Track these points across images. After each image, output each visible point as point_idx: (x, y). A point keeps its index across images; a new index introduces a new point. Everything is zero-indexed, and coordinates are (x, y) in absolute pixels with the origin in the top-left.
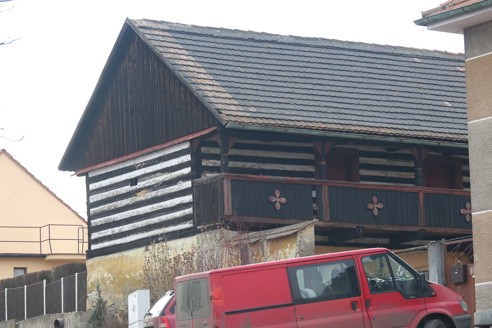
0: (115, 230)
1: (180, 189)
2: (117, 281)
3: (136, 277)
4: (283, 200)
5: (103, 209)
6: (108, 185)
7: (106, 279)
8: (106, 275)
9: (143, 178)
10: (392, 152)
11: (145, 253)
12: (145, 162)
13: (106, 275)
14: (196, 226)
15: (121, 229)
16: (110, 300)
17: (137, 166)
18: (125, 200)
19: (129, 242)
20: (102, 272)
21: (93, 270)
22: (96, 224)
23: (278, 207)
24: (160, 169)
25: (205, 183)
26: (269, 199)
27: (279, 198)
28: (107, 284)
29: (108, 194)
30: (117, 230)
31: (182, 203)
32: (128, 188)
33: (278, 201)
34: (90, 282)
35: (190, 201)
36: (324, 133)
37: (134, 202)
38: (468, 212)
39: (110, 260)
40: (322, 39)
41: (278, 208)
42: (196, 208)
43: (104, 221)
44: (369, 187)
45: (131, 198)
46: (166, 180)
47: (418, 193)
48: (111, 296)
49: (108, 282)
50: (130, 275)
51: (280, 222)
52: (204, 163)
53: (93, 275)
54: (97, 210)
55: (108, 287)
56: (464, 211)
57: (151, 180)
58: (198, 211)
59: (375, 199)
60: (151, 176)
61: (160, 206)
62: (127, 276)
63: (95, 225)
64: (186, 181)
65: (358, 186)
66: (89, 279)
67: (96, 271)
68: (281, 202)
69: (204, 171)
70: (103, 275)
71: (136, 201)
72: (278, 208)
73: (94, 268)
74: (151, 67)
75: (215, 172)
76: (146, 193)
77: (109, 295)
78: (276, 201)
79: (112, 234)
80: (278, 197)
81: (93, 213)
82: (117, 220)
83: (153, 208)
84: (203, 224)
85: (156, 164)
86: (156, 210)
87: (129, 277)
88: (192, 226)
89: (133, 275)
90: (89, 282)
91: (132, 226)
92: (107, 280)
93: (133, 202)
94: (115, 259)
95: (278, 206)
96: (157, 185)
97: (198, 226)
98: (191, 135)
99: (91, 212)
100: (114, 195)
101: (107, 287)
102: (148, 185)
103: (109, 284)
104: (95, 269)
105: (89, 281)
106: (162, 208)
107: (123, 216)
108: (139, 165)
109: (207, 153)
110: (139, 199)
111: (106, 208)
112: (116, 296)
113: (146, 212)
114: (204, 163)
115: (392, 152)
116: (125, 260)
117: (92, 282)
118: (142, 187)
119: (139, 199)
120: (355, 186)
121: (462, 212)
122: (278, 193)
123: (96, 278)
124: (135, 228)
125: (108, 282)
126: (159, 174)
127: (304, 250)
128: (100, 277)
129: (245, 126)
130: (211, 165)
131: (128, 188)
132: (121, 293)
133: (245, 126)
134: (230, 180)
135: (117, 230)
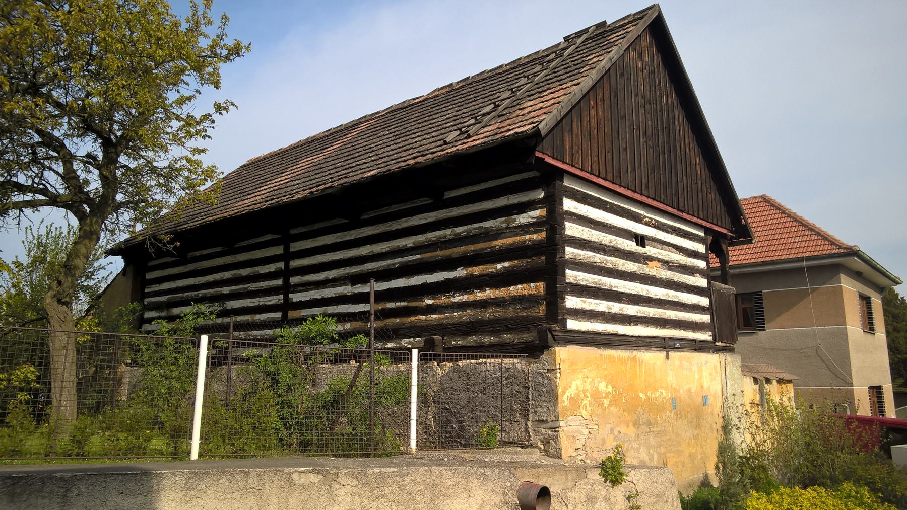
5: (592, 259)
7: (604, 395)
8: (602, 386)
13: (602, 386)
16: (612, 437)
21: (574, 371)
22: (575, 280)
28: (606, 405)
34: (568, 396)
43: (594, 283)
48: (612, 430)
49: (606, 402)
50: (646, 394)
55: (607, 410)
57: (665, 253)
62: (641, 395)
63: (573, 282)
67: (581, 375)
77: (609, 426)
79: (607, 311)
81: (571, 256)
85: (668, 232)
89: (651, 395)
103: (609, 406)
104: (578, 371)
105: (564, 392)
107: (625, 287)
108: (647, 219)
112: (623, 429)
116: (638, 366)
117: (573, 396)
124: (644, 315)
125: (606, 402)
128: (590, 390)
132: (631, 425)
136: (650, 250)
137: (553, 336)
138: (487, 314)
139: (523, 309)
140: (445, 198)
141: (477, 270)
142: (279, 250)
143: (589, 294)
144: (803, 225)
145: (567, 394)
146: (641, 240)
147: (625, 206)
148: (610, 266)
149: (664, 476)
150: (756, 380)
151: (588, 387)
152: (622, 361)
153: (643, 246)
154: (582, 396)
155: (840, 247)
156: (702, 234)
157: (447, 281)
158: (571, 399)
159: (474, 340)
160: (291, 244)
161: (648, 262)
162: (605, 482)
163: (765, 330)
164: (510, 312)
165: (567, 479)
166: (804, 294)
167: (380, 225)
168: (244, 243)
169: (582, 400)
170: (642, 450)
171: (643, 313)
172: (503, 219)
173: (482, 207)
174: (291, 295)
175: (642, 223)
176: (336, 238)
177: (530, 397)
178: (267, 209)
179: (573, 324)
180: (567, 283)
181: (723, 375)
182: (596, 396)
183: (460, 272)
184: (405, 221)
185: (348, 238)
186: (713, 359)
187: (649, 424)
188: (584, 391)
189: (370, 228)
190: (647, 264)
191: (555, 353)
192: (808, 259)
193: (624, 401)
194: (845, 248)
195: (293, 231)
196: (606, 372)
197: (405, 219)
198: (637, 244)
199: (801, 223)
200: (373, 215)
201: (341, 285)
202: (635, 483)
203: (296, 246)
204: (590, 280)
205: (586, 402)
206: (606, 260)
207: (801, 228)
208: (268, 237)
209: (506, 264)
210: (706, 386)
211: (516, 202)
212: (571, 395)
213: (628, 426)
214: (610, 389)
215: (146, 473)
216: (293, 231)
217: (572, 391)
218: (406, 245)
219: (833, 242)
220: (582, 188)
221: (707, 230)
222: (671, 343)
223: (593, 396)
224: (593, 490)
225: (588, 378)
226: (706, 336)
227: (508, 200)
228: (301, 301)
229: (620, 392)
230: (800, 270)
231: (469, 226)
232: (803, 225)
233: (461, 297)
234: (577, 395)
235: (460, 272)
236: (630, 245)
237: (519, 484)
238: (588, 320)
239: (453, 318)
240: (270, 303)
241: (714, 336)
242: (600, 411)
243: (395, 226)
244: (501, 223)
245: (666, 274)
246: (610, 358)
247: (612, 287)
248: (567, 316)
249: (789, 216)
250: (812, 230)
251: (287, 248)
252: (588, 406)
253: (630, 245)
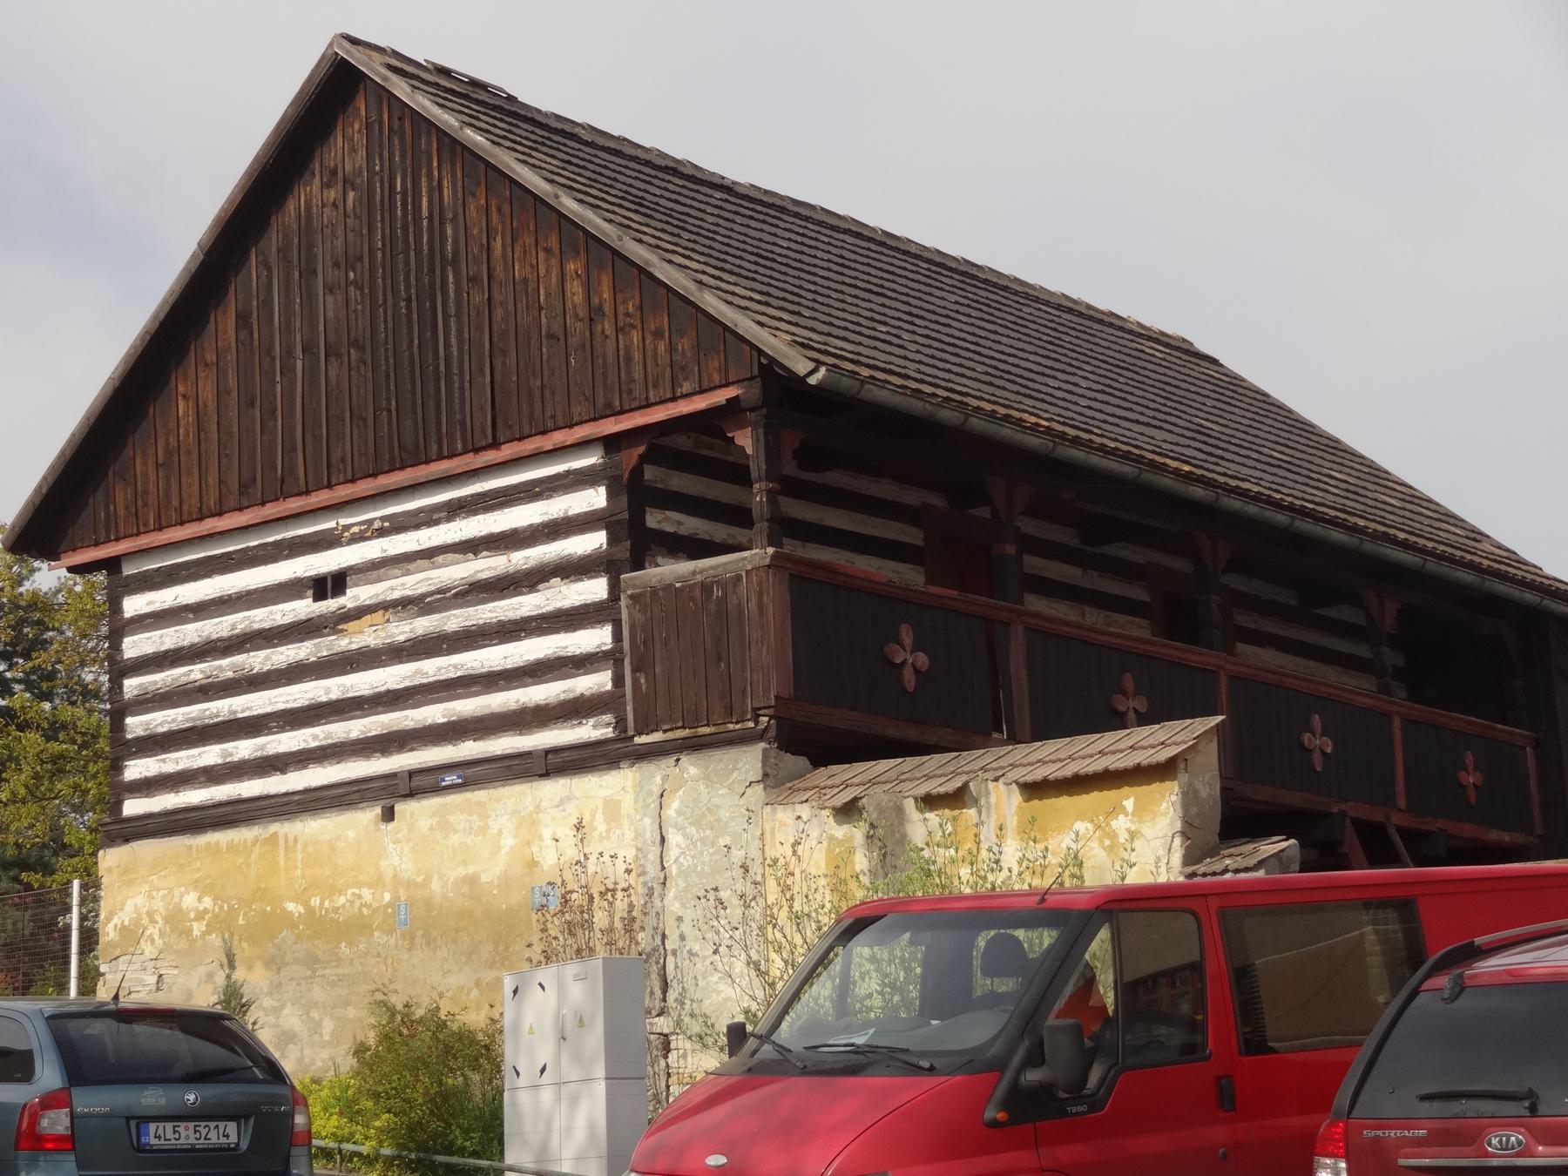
0: (236, 748)
1: (550, 608)
2: (241, 922)
3: (336, 910)
4: (922, 659)
5: (184, 680)
6: (207, 598)
7: (192, 915)
8: (190, 900)
9: (375, 574)
10: (1091, 549)
11: (379, 829)
12: (383, 519)
13: (190, 900)
14: (631, 733)
15: (263, 747)
17: (346, 534)
18: (289, 647)
19: (301, 788)
20: (171, 890)
21: (129, 883)
22: (146, 730)
23: (909, 682)
24: (457, 540)
25: (678, 585)
26: (887, 650)
27: (912, 653)
29: (206, 627)
30: (244, 749)
31: (562, 654)
32: (303, 608)
33: (910, 661)
34: (116, 926)
35: (598, 647)
36: (1051, 444)
37: (331, 652)
38: (1318, 742)
39: (214, 850)
40: (822, 209)
41: (911, 687)
42: (635, 671)
43: (188, 720)
44: (1116, 641)
45: (319, 640)
46: (484, 575)
47: (1215, 672)
49: (198, 928)
50: (306, 904)
51: (912, 734)
52: (655, 519)
53: (129, 902)
54: (155, 683)
55: (200, 943)
56: (1309, 739)
57: (410, 580)
58: (643, 681)
59: (1128, 681)
60: (412, 566)
61: (455, 666)
62: (291, 906)
63: (142, 733)
64: (582, 580)
65: (1093, 635)
68: (918, 666)
69: (653, 547)
70: (176, 899)
71: (337, 649)
72: (911, 687)
73: (137, 879)
74: (425, 200)
75: (680, 554)
76: (388, 621)
78: (904, 663)
79: (220, 761)
80: (909, 649)
81: (135, 692)
82: (247, 714)
83: (418, 672)
84: (665, 727)
85: (437, 522)
86: (431, 680)
87: (302, 911)
88: (611, 735)
89: (322, 903)
90: (111, 926)
91: (315, 737)
92: (196, 919)
93: (325, 654)
94: (232, 847)
95: (909, 677)
96: (439, 596)
97: (640, 734)
98: (613, 418)
99: (125, 690)
100: (236, 632)
101: (195, 940)
102: (396, 595)
103: (204, 934)
104: (138, 881)
105: (109, 919)
106: (459, 674)
107: (273, 700)
109: (659, 486)
110: (351, 643)
111: (194, 676)
113: (383, 689)
114: (655, 519)
115: (1091, 549)
116: (282, 852)
117: (126, 923)
118: (367, 603)
119: (351, 643)
120: (1085, 633)
121: (1306, 743)
122: (907, 637)
123: (146, 909)
124: (330, 741)
125: (198, 928)
126: (450, 557)
127: (1197, 822)
128: (162, 910)
129: (867, 386)
130: (669, 528)
131: (303, 608)
133: (867, 386)
134: (787, 575)
135: (244, 749)
145: (116, 920)
147: (278, 537)
148: (230, 674)
151: (159, 905)
154: (145, 921)
158: (123, 930)
169: (145, 929)
170: (286, 1011)
171: (325, 738)
182: (176, 921)
186: (619, 784)
187: (312, 961)
188: (150, 914)
193: (241, 922)
204: (180, 718)
205: (153, 931)
206: (220, 667)
212: (123, 921)
214: (207, 902)
217: (125, 916)
220: (163, 561)
222: (427, 780)
223: (167, 920)
225: (159, 890)
229: (231, 908)
234: (136, 922)
238: (171, 791)
241: (620, 724)
242: (183, 944)
245: (403, 630)
247: (235, 712)
252: (156, 937)
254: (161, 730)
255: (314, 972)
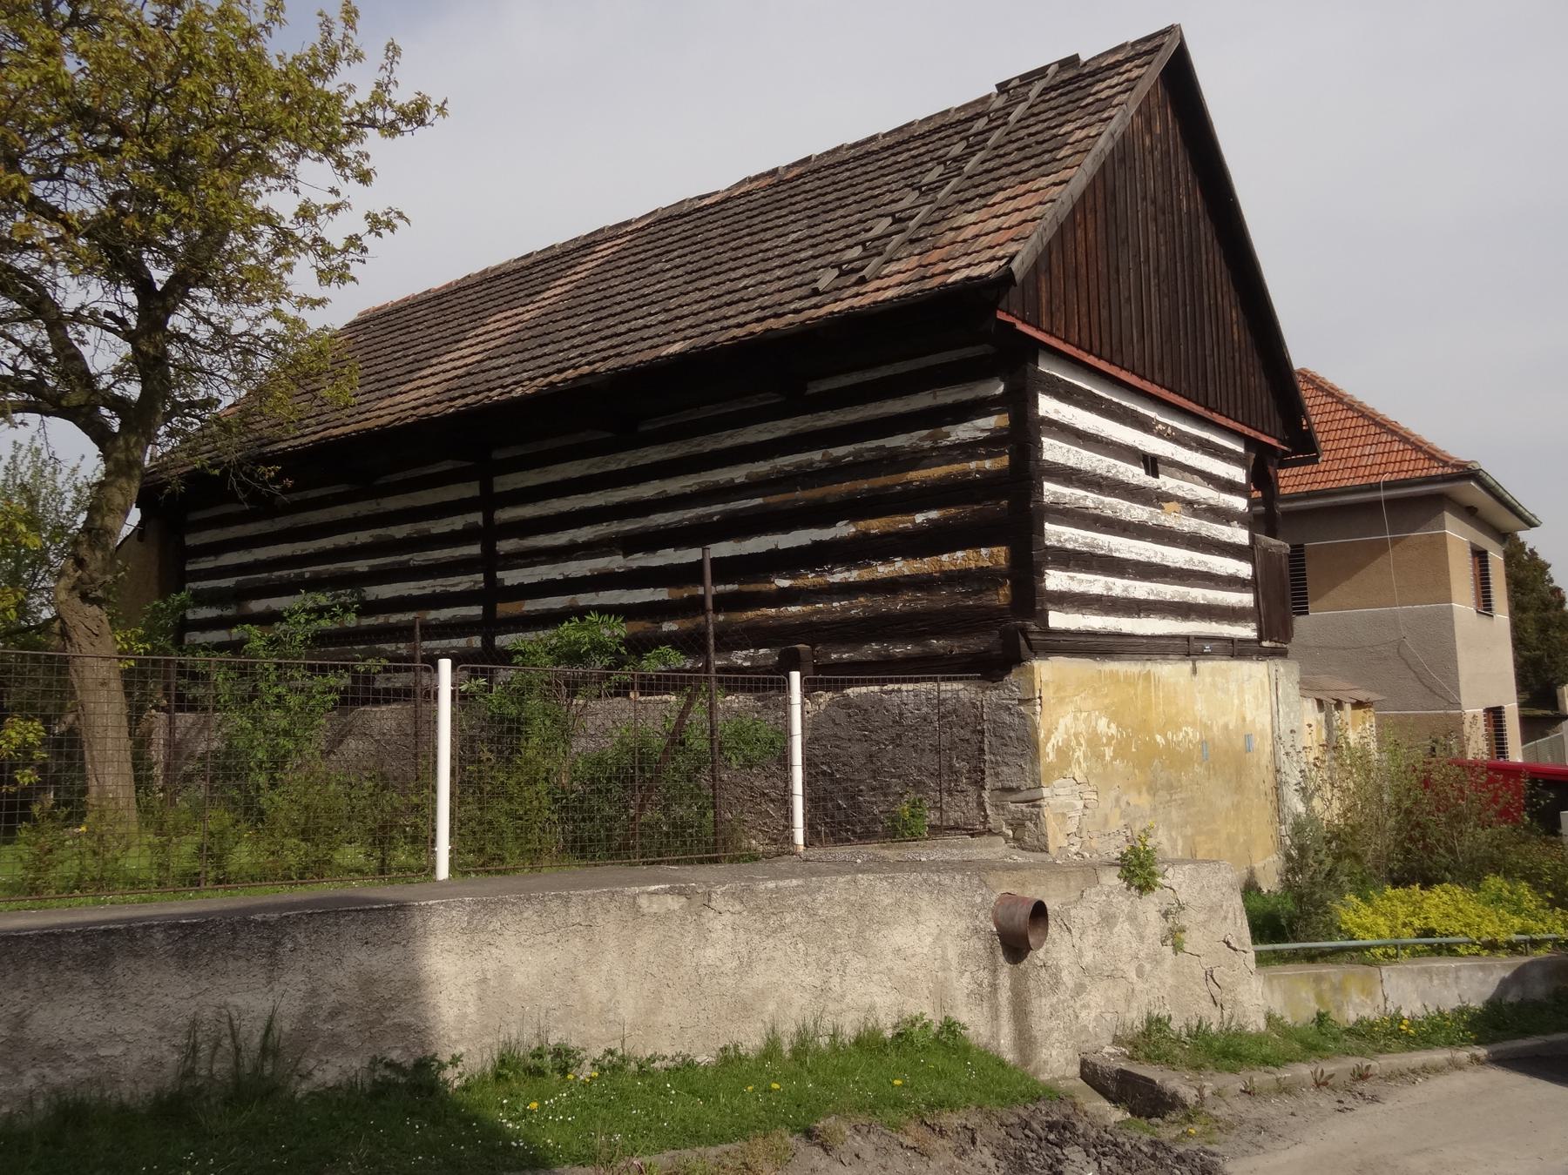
16: (1117, 811)
21: (1061, 701)
28: (1107, 758)
43: (1086, 544)
48: (1117, 800)
49: (1109, 753)
53: (1061, 721)
55: (1110, 767)
57: (1187, 485)
62: (1159, 738)
66: (1050, 733)
67: (1071, 708)
77: (1113, 794)
85: (1191, 448)
90: (1050, 745)
92: (1106, 745)
103: (1114, 758)
105: (1048, 739)
108: (1160, 427)
111: (1089, 503)
112: (1133, 798)
125: (1109, 753)
132: (1144, 789)
136: (1166, 483)
137: (1028, 640)
138: (900, 604)
139: (966, 595)
140: (810, 392)
141: (875, 526)
142: (470, 490)
143: (1077, 565)
144: (1377, 424)
145: (1053, 741)
146: (1152, 464)
148: (1109, 513)
149: (1220, 875)
150: (1320, 703)
151: (1082, 727)
152: (1129, 681)
153: (1155, 474)
154: (1073, 743)
155: (1446, 464)
156: (1240, 449)
157: (818, 545)
159: (874, 651)
160: (496, 479)
161: (1164, 504)
162: (1128, 889)
163: (1307, 613)
164: (943, 599)
165: (1068, 887)
166: (1382, 548)
167: (678, 444)
168: (398, 477)
169: (1074, 751)
172: (925, 432)
173: (879, 411)
174: (499, 574)
175: (1152, 434)
176: (589, 468)
177: (986, 748)
178: (457, 414)
179: (1058, 620)
180: (1047, 548)
181: (1274, 698)
182: (1094, 742)
183: (844, 530)
184: (729, 436)
185: (613, 467)
186: (1255, 672)
188: (1076, 735)
189: (660, 448)
190: (1162, 508)
191: (1032, 671)
192: (1389, 485)
194: (1454, 466)
195: (498, 455)
196: (1107, 701)
197: (728, 432)
198: (1147, 473)
199: (1374, 419)
200: (663, 424)
201: (603, 555)
202: (1175, 888)
203: (506, 483)
205: (1079, 754)
206: (1103, 502)
207: (1373, 429)
208: (447, 466)
209: (934, 514)
210: (1249, 718)
211: (949, 400)
213: (1140, 793)
214: (1113, 730)
215: (401, 906)
216: (498, 455)
218: (733, 480)
219: (1432, 456)
221: (1249, 442)
222: (1197, 645)
223: (1090, 743)
224: (1110, 904)
226: (1247, 631)
227: (935, 398)
228: (521, 585)
230: (1374, 506)
231: (858, 446)
232: (1377, 424)
233: (846, 574)
234: (1067, 742)
235: (844, 530)
236: (1135, 474)
237: (994, 898)
238: (1078, 611)
239: (830, 612)
240: (458, 589)
241: (1259, 630)
242: (1099, 770)
243: (709, 444)
244: (922, 439)
245: (1189, 524)
246: (1113, 675)
247: (1111, 550)
248: (1049, 606)
249: (1350, 407)
250: (1393, 432)
251: (486, 487)
253: (1135, 474)
254: (1069, 546)
255: (1171, 795)
